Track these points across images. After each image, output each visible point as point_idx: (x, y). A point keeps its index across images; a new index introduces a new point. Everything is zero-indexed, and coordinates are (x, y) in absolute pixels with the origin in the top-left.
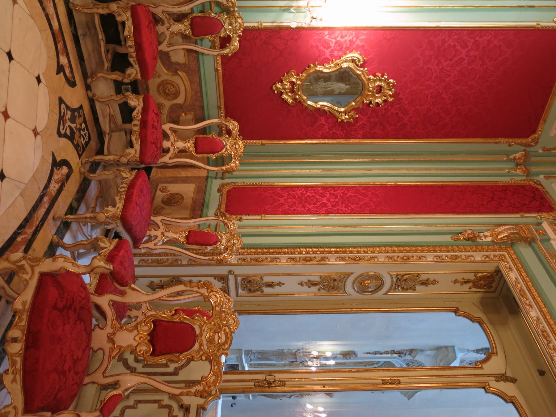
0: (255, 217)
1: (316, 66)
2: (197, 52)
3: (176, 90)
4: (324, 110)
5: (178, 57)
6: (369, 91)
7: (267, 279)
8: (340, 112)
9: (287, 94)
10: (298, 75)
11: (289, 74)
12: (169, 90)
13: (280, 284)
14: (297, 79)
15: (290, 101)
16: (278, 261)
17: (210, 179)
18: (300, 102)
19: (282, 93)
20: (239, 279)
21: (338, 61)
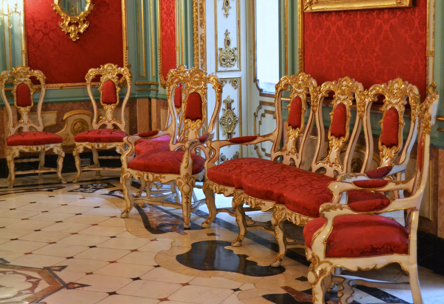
0: (177, 56)
1: (55, 5)
2: (44, 104)
3: (79, 121)
5: (51, 118)
7: (221, 44)
9: (80, 28)
10: (63, 20)
12: (80, 127)
13: (227, 34)
14: (66, 20)
15: (85, 26)
16: (203, 35)
17: (158, 96)
18: (86, 17)
19: (79, 33)
20: (220, 68)
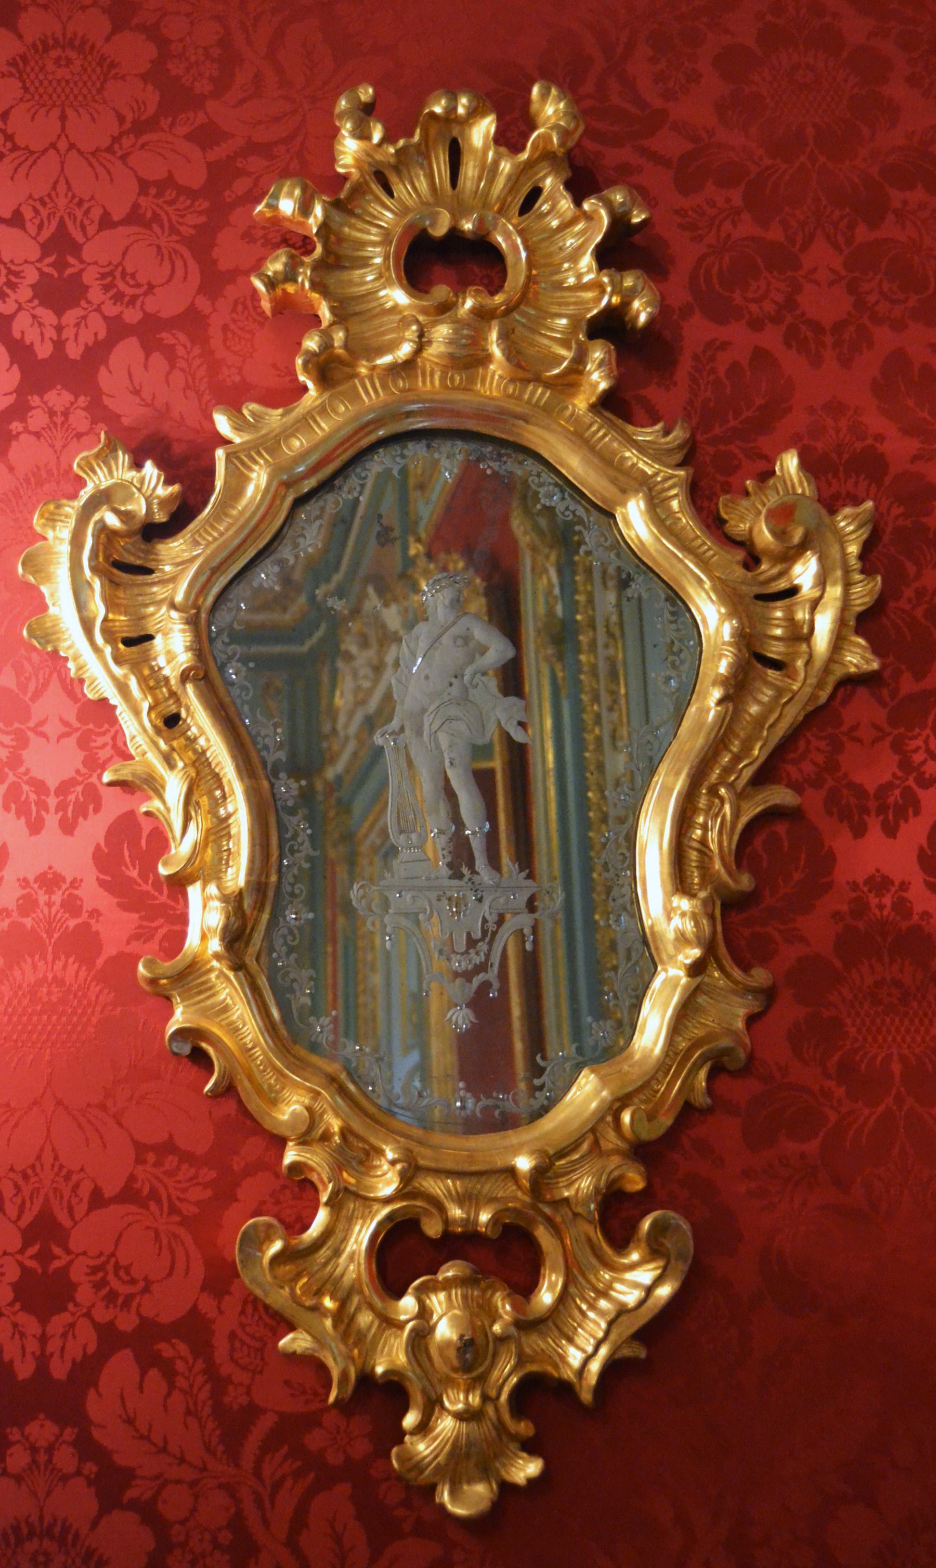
1: (190, 976)
4: (748, 844)
6: (468, 359)
8: (753, 658)
9: (557, 1321)
11: (279, 1298)
14: (348, 1200)
15: (638, 1282)
19: (542, 1393)
21: (135, 729)
